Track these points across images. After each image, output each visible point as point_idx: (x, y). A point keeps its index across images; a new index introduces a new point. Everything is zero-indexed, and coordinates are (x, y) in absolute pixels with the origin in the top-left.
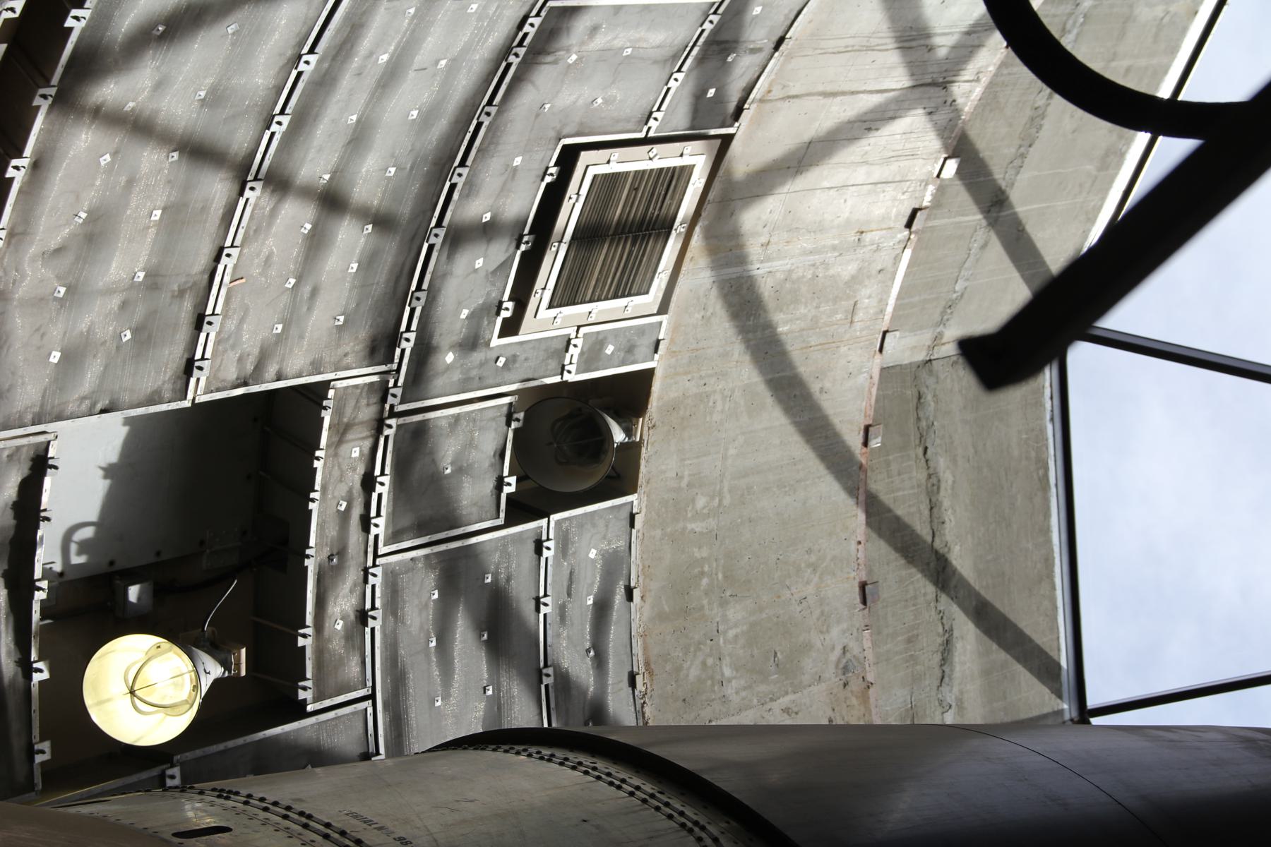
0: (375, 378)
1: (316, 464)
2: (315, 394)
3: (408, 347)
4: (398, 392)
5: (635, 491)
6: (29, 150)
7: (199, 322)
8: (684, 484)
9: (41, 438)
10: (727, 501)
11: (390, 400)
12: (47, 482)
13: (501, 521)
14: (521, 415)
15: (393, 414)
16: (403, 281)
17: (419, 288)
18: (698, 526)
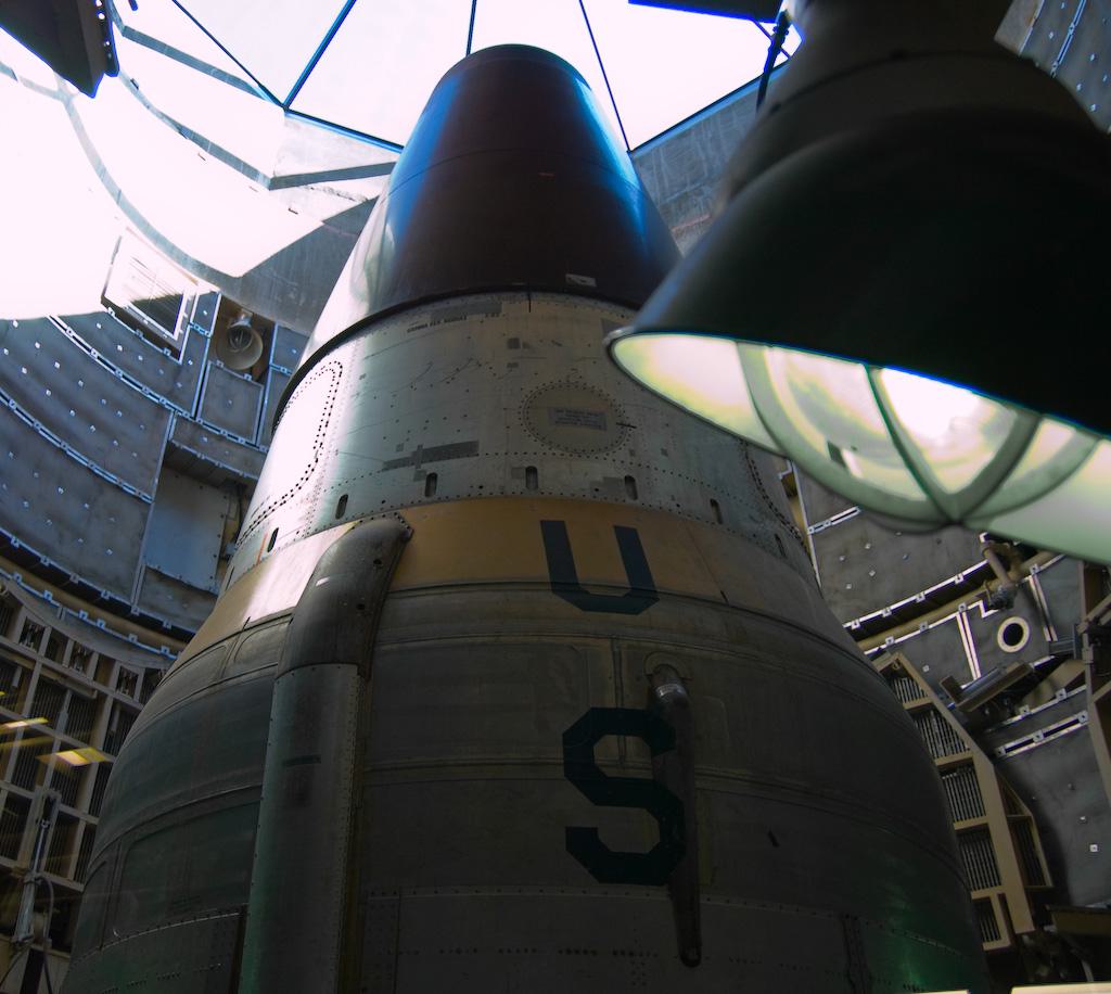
0: (175, 421)
1: (203, 458)
2: (171, 448)
3: (166, 401)
4: (185, 412)
5: (274, 324)
6: (10, 535)
7: (118, 488)
8: (280, 301)
9: (144, 569)
10: (296, 284)
11: (188, 417)
12: (165, 572)
13: (263, 387)
14: (218, 362)
15: (195, 419)
16: (135, 394)
17: (141, 388)
18: (302, 301)
